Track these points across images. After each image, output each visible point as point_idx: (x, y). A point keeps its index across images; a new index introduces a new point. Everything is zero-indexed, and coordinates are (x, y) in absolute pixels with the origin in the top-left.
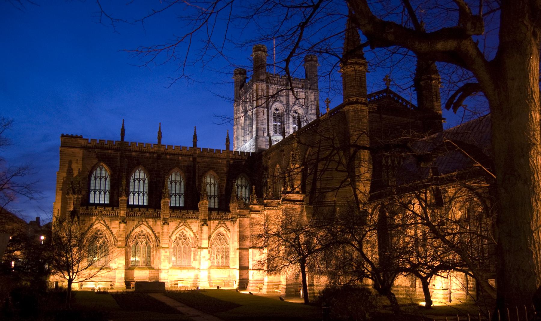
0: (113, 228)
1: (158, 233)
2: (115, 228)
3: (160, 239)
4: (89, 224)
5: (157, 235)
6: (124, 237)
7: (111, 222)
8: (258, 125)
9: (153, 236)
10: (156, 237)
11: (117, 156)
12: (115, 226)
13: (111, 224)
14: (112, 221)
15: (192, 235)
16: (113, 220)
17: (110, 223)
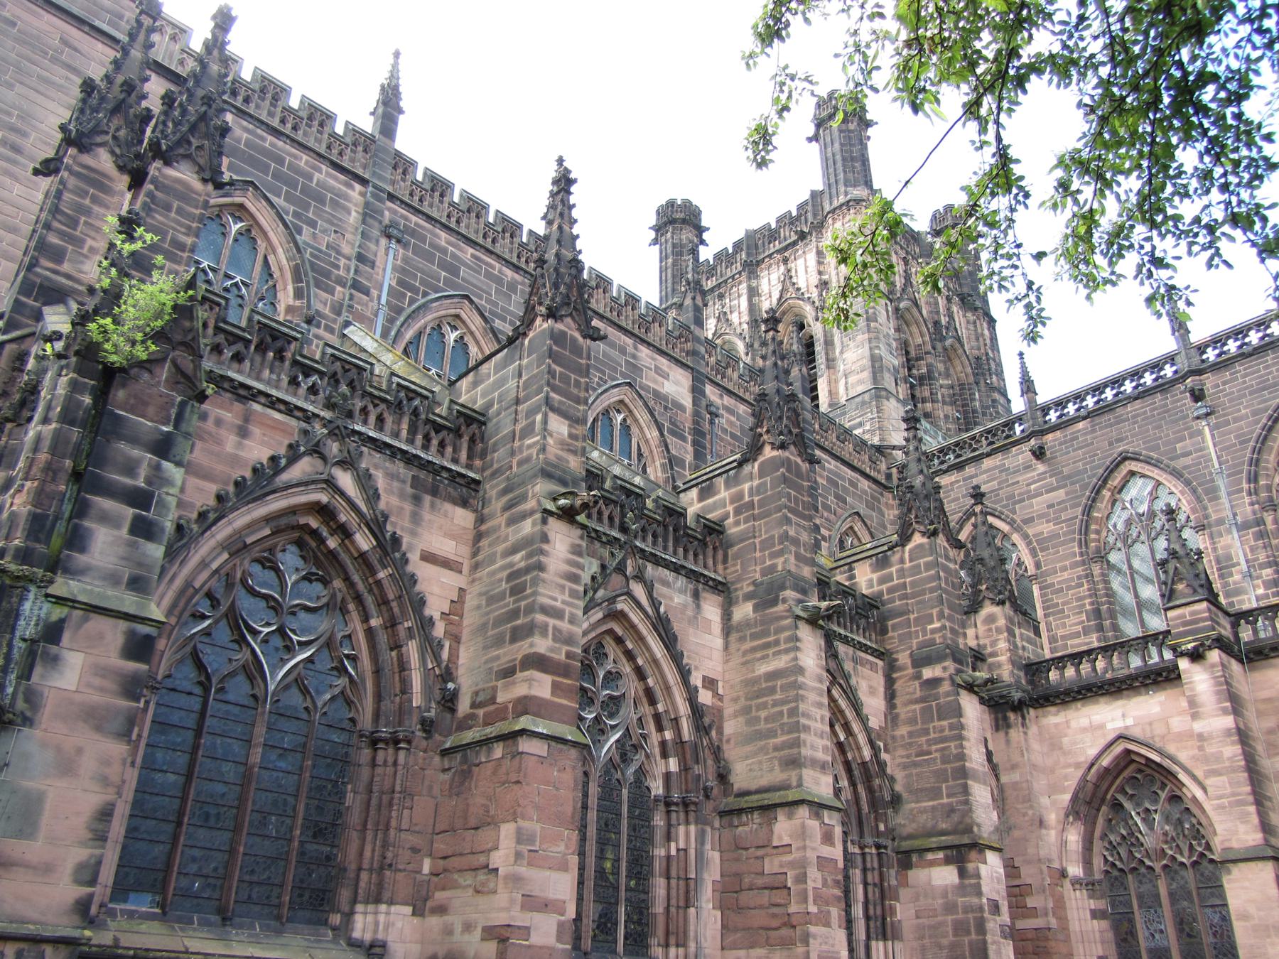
0: (428, 557)
1: (710, 683)
2: (446, 564)
3: (720, 731)
4: (235, 460)
5: (705, 697)
6: (569, 640)
7: (417, 500)
8: (878, 347)
9: (683, 708)
10: (697, 711)
11: (347, 198)
12: (446, 547)
13: (416, 518)
14: (427, 499)
15: (867, 753)
16: (434, 492)
17: (408, 507)
